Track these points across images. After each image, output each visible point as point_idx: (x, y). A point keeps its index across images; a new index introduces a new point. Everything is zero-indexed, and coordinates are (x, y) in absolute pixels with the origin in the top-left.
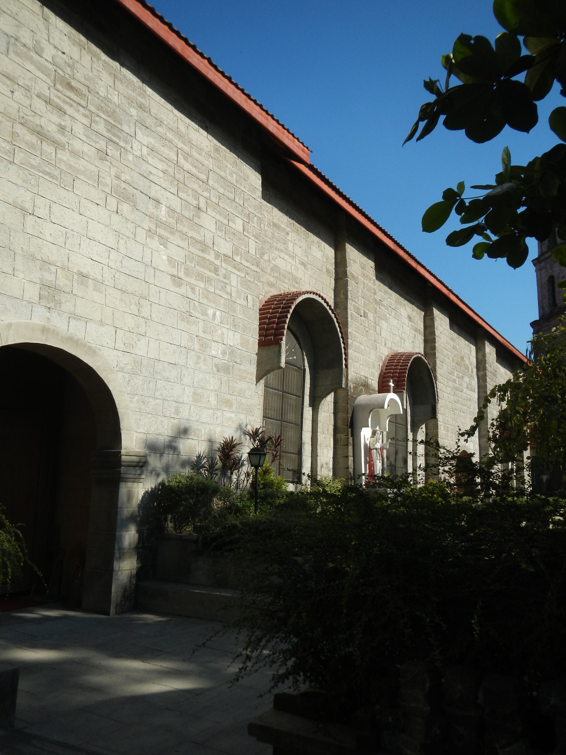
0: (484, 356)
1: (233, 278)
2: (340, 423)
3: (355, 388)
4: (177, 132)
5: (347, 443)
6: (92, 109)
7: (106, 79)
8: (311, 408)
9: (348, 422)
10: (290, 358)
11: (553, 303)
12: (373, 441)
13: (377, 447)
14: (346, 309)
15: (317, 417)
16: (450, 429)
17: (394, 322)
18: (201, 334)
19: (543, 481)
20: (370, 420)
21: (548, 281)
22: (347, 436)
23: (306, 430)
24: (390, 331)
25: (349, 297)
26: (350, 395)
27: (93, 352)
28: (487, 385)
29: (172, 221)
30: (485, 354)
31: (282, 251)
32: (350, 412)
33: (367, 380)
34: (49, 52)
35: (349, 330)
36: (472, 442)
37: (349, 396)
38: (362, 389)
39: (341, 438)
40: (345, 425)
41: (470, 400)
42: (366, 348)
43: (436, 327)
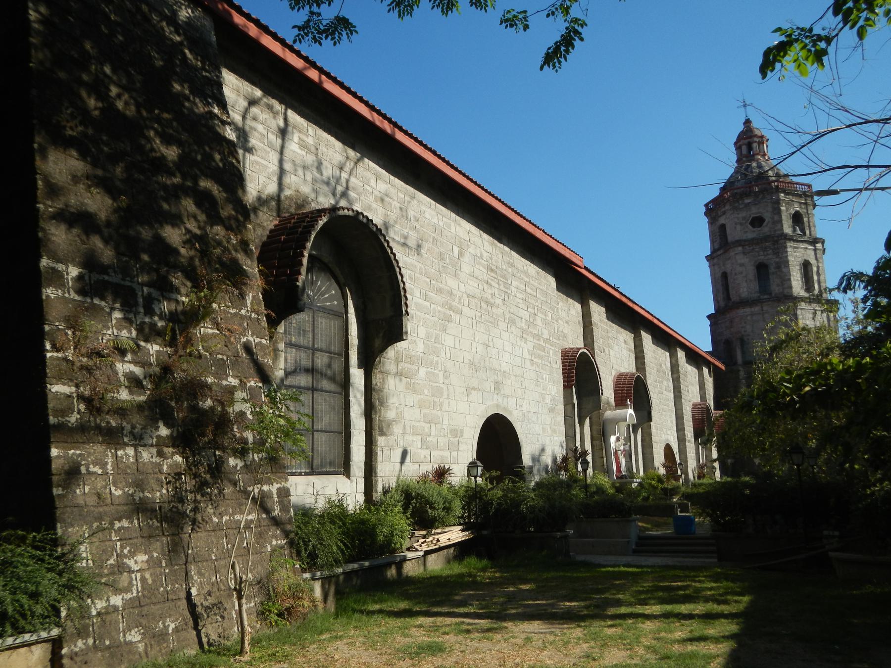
0: (677, 361)
1: (551, 351)
2: (595, 433)
4: (524, 272)
6: (499, 278)
7: (500, 256)
11: (728, 297)
14: (593, 349)
17: (616, 348)
18: (543, 392)
27: (511, 413)
29: (527, 327)
34: (485, 254)
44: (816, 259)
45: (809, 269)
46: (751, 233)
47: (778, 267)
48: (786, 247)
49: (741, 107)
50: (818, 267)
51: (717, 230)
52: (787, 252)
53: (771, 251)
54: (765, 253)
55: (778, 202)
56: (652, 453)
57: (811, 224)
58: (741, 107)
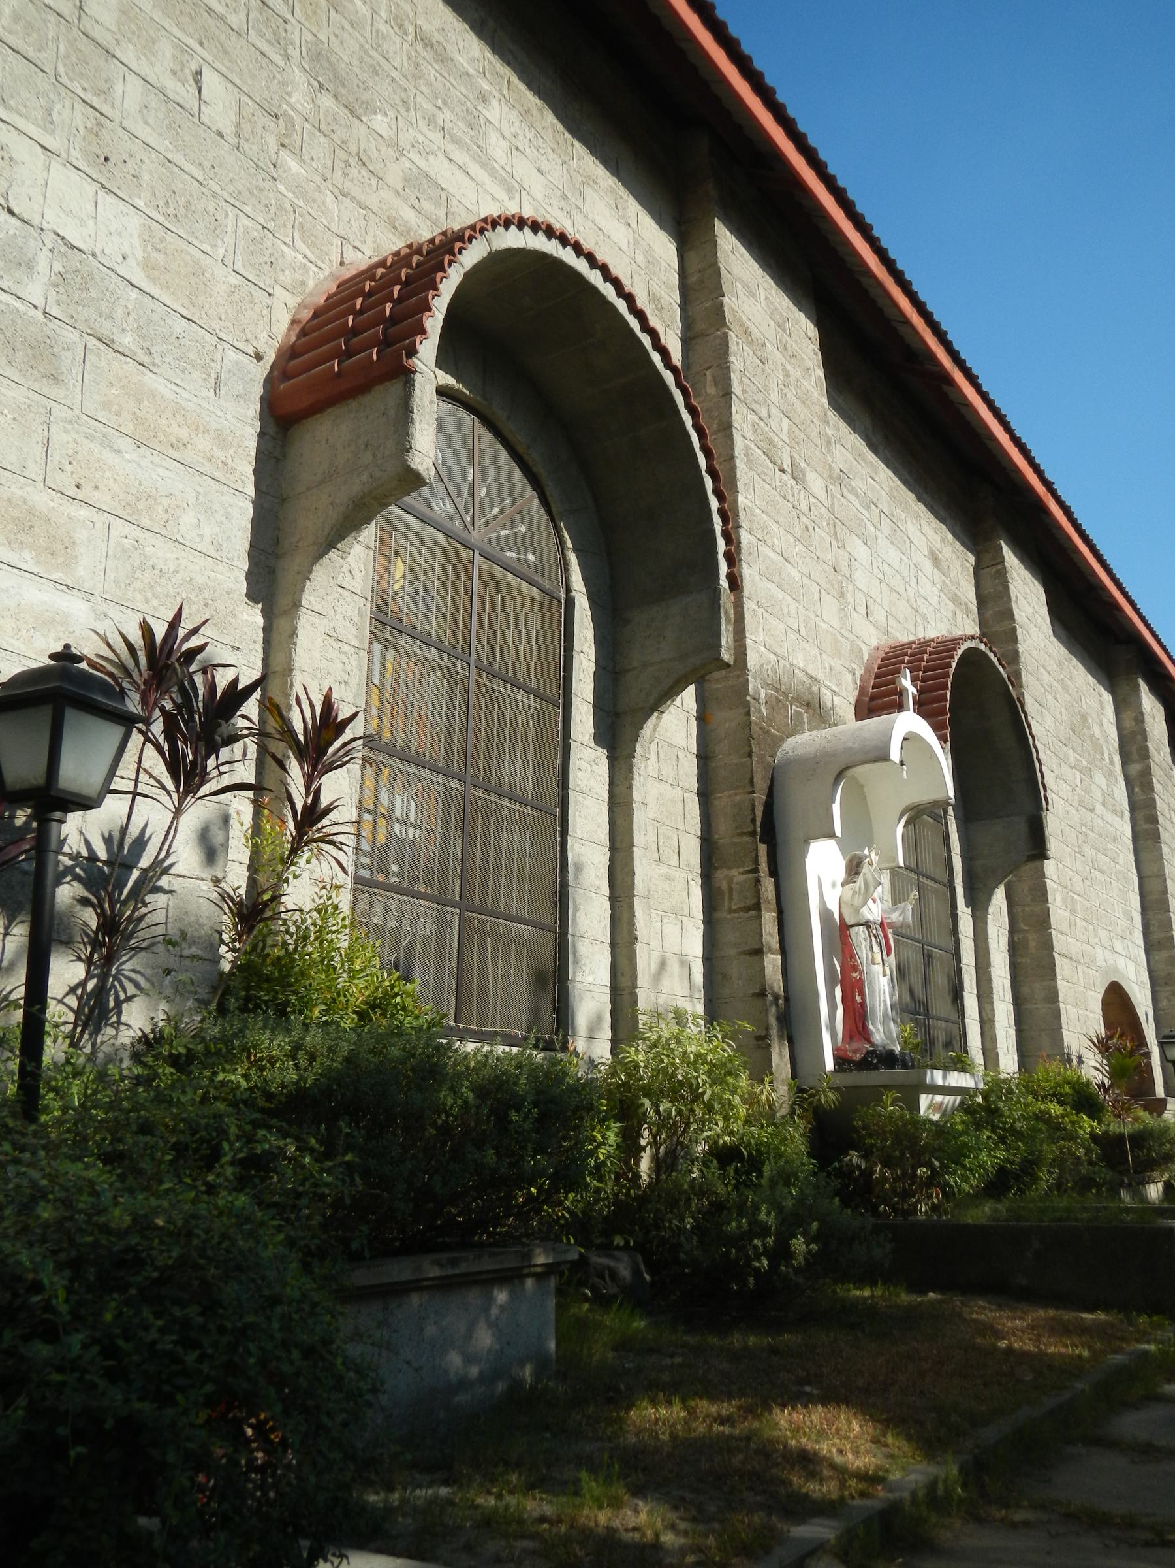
0: (1140, 719)
2: (724, 828)
3: (776, 704)
5: (754, 901)
8: (602, 754)
9: (753, 821)
10: (505, 532)
12: (854, 893)
13: (871, 918)
15: (630, 787)
16: (1078, 907)
17: (893, 555)
20: (836, 808)
22: (752, 875)
23: (585, 836)
24: (881, 576)
25: (737, 388)
26: (756, 724)
28: (1154, 800)
30: (1142, 714)
31: (456, 141)
32: (761, 784)
33: (815, 688)
35: (741, 498)
36: (1130, 958)
37: (754, 728)
38: (799, 714)
39: (730, 881)
40: (743, 834)
41: (1115, 840)
42: (806, 581)
43: (1013, 599)
56: (1053, 997)
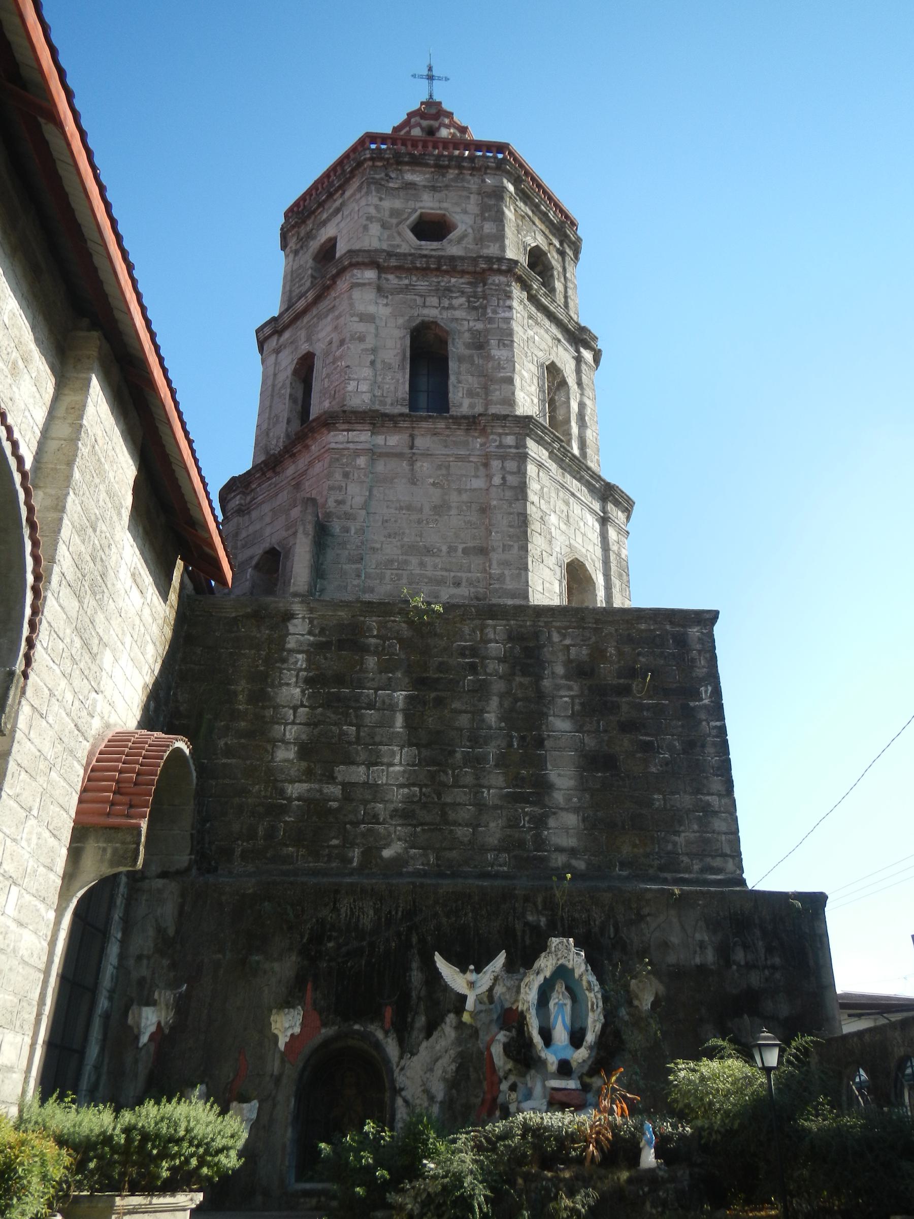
19: (137, 1038)
21: (296, 372)
44: (580, 384)
45: (560, 398)
46: (408, 242)
47: (480, 344)
48: (509, 297)
49: (421, 77)
50: (582, 405)
51: (311, 263)
52: (510, 308)
53: (462, 300)
54: (446, 303)
55: (498, 194)
57: (571, 304)
58: (421, 77)
